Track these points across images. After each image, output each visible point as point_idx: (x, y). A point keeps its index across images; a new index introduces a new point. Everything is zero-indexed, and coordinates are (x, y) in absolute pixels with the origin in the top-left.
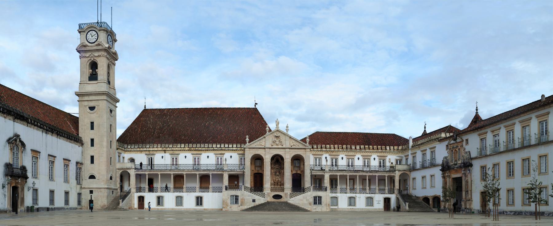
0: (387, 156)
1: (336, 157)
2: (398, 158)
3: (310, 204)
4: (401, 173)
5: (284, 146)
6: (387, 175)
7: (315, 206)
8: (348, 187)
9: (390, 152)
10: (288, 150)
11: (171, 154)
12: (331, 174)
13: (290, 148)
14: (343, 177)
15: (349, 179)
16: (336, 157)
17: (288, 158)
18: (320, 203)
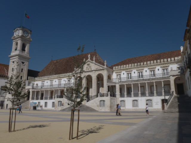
0: (169, 66)
1: (130, 72)
2: (179, 66)
3: (98, 106)
4: (175, 77)
5: (92, 70)
6: (162, 80)
7: (101, 108)
8: (140, 92)
9: (171, 63)
10: (94, 71)
11: (58, 80)
12: (120, 84)
13: (95, 70)
14: (136, 85)
15: (141, 87)
16: (130, 72)
17: (94, 76)
18: (104, 105)
